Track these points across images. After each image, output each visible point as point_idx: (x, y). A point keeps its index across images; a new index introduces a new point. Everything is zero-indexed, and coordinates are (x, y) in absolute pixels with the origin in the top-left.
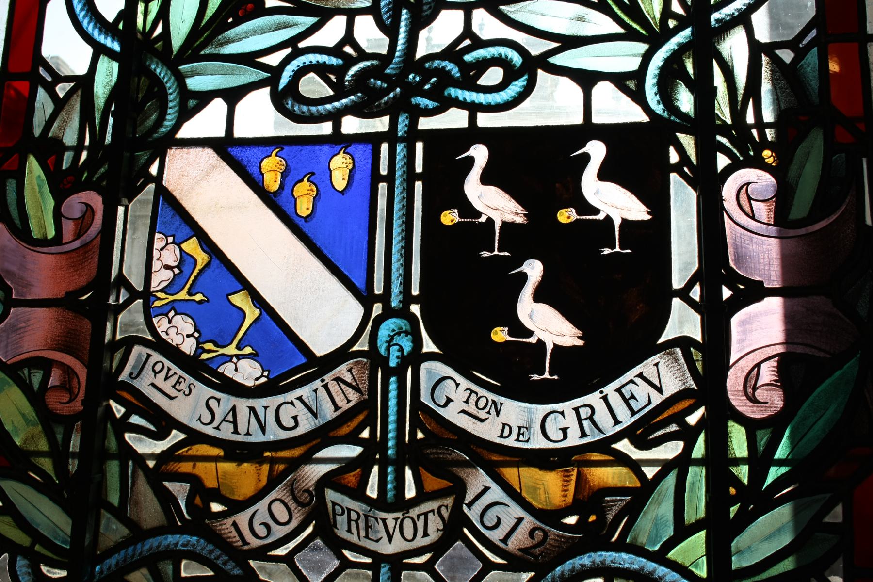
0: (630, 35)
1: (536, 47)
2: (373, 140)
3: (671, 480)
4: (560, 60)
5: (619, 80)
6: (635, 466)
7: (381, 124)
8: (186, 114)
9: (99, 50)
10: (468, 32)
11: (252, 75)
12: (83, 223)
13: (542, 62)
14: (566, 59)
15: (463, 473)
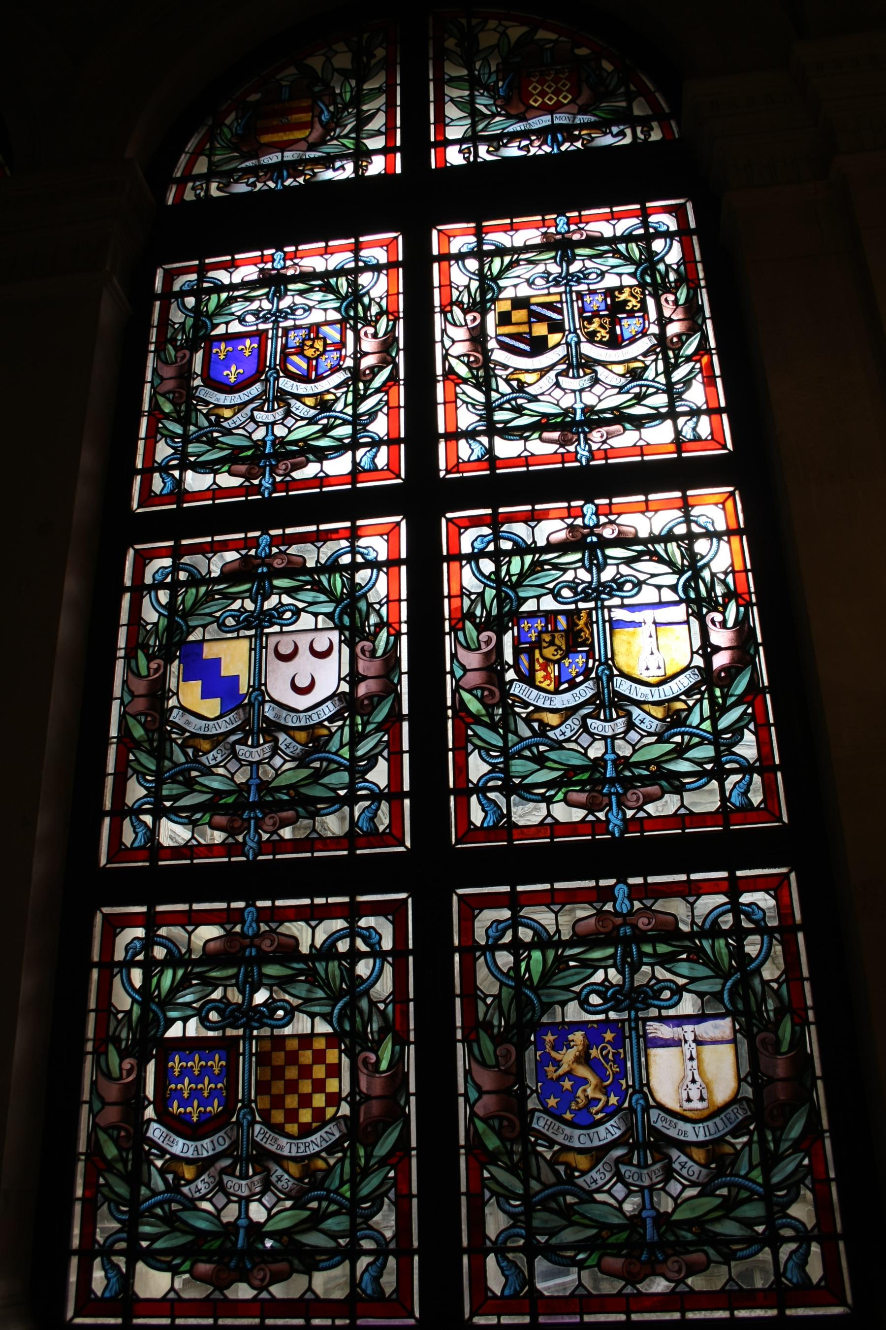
0: (331, 601)
1: (301, 605)
2: (250, 637)
3: (339, 732)
4: (309, 609)
5: (325, 614)
6: (328, 728)
7: (253, 632)
8: (189, 633)
9: (160, 614)
10: (280, 602)
11: (211, 619)
12: (156, 670)
13: (303, 610)
14: (310, 609)
15: (277, 734)
